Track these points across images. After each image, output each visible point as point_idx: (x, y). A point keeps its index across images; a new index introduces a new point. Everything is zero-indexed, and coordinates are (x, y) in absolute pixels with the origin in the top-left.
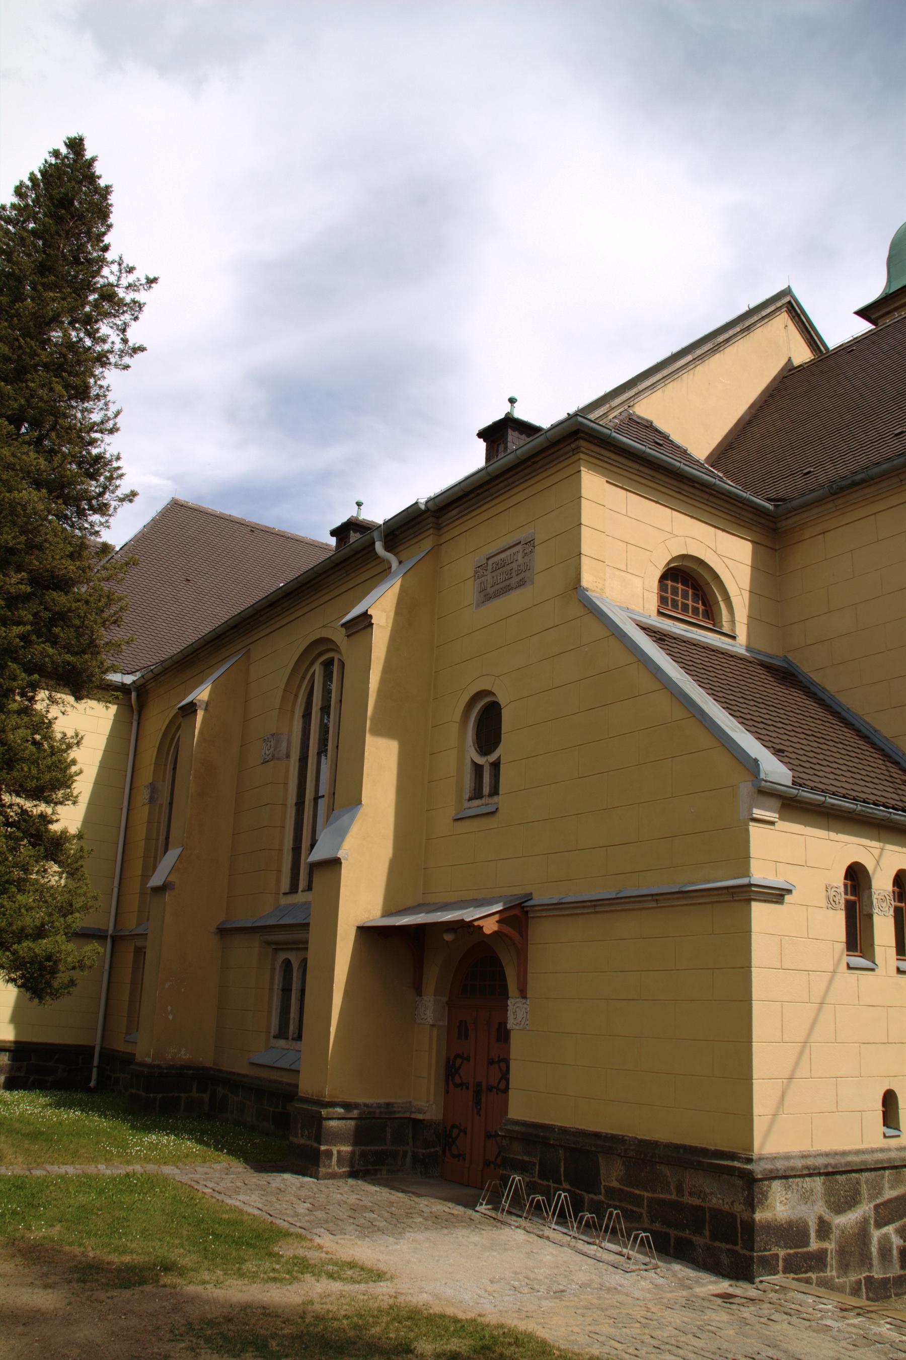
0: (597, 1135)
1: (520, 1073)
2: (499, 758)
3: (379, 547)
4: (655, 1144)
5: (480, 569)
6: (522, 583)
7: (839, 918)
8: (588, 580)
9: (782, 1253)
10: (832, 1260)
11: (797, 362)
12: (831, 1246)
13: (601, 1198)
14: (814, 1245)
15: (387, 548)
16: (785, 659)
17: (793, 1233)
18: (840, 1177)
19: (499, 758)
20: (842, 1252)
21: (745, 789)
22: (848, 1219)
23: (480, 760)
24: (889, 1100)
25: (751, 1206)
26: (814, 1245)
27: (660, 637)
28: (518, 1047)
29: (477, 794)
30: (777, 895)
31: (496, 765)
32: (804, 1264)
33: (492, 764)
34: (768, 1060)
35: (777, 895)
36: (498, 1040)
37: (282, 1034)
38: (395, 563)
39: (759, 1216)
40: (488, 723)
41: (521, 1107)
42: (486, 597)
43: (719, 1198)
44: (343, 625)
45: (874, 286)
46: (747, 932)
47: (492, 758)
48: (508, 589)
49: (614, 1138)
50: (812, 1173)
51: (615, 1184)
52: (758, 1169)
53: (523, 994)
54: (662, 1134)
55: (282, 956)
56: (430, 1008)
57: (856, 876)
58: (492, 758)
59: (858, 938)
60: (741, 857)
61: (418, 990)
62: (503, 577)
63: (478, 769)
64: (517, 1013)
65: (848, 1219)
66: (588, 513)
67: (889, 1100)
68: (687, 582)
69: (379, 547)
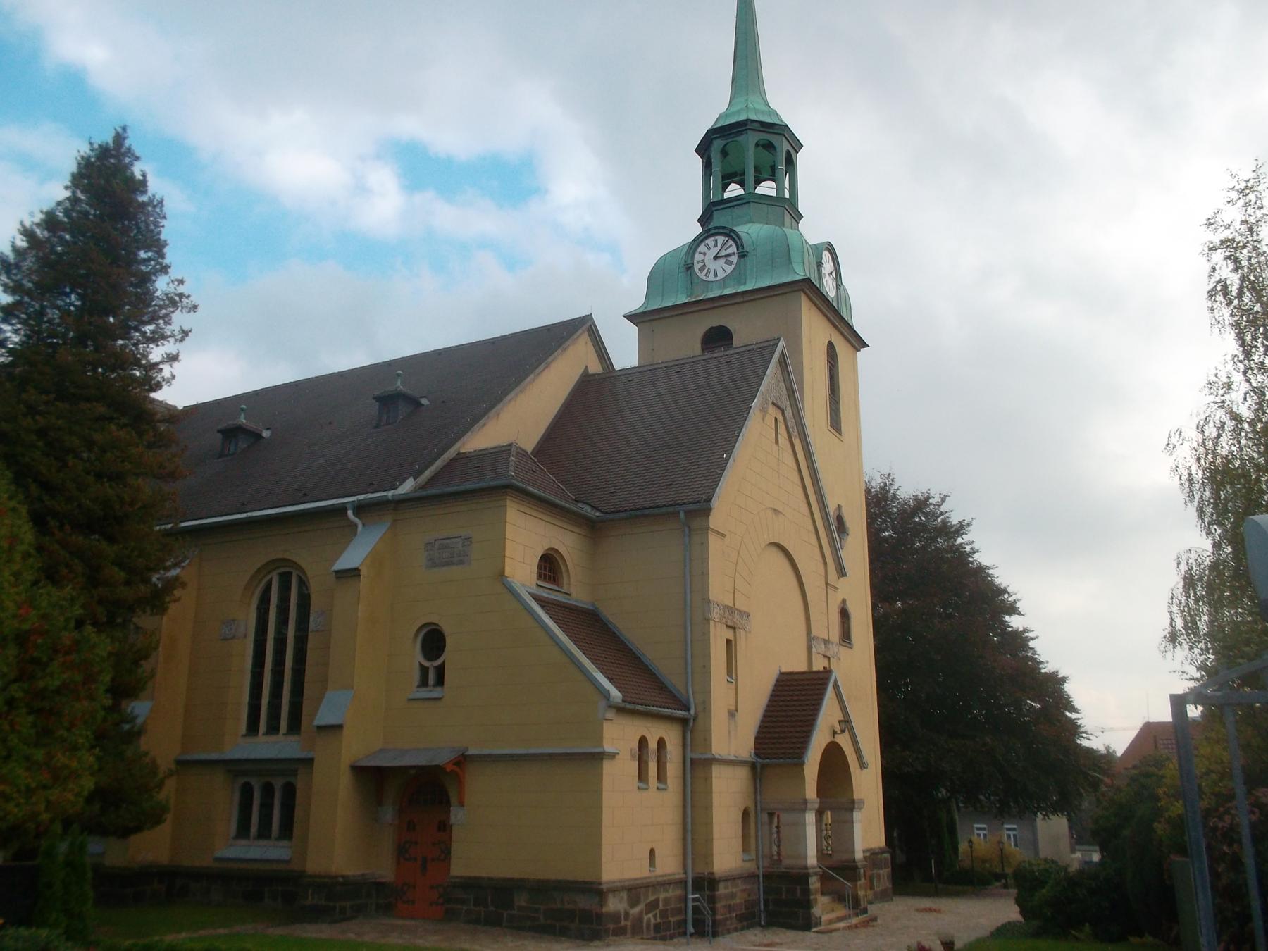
0: (512, 879)
1: (457, 849)
2: (444, 663)
3: (350, 513)
4: (548, 881)
5: (429, 546)
6: (461, 563)
7: (635, 765)
8: (508, 572)
9: (611, 926)
10: (629, 931)
11: (591, 371)
12: (629, 923)
13: (515, 912)
14: (623, 923)
15: (356, 514)
16: (593, 605)
17: (615, 917)
18: (634, 890)
19: (444, 663)
20: (633, 927)
21: (602, 704)
22: (636, 910)
23: (427, 664)
24: (652, 852)
25: (602, 906)
26: (623, 923)
27: (536, 598)
28: (456, 832)
29: (424, 682)
30: (613, 756)
31: (440, 671)
32: (620, 932)
33: (436, 667)
34: (609, 835)
35: (613, 756)
36: (439, 829)
37: (264, 834)
38: (360, 527)
39: (604, 910)
40: (434, 641)
41: (460, 867)
42: (433, 564)
43: (583, 902)
44: (337, 572)
45: (637, 301)
46: (600, 775)
47: (438, 662)
48: (452, 563)
49: (521, 880)
50: (623, 888)
51: (524, 904)
52: (604, 887)
53: (461, 804)
54: (551, 875)
55: (241, 780)
56: (388, 813)
57: (643, 742)
58: (438, 662)
59: (642, 775)
60: (599, 739)
61: (380, 803)
62: (447, 555)
63: (424, 671)
64: (457, 816)
65: (636, 910)
66: (510, 532)
67: (652, 852)
68: (550, 565)
69: (350, 513)
